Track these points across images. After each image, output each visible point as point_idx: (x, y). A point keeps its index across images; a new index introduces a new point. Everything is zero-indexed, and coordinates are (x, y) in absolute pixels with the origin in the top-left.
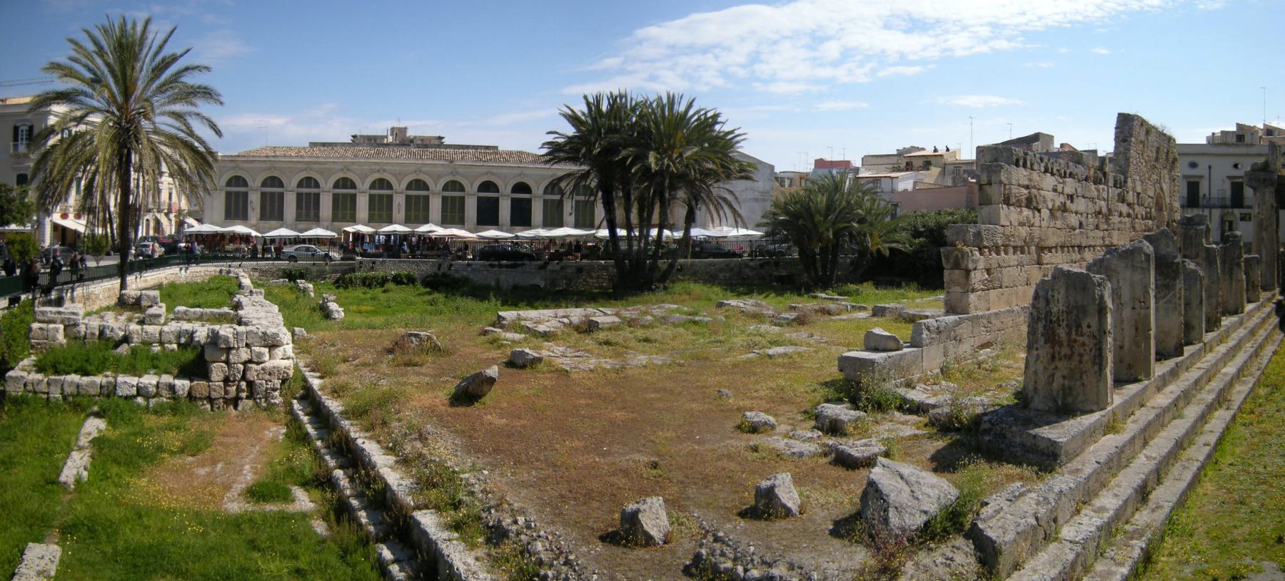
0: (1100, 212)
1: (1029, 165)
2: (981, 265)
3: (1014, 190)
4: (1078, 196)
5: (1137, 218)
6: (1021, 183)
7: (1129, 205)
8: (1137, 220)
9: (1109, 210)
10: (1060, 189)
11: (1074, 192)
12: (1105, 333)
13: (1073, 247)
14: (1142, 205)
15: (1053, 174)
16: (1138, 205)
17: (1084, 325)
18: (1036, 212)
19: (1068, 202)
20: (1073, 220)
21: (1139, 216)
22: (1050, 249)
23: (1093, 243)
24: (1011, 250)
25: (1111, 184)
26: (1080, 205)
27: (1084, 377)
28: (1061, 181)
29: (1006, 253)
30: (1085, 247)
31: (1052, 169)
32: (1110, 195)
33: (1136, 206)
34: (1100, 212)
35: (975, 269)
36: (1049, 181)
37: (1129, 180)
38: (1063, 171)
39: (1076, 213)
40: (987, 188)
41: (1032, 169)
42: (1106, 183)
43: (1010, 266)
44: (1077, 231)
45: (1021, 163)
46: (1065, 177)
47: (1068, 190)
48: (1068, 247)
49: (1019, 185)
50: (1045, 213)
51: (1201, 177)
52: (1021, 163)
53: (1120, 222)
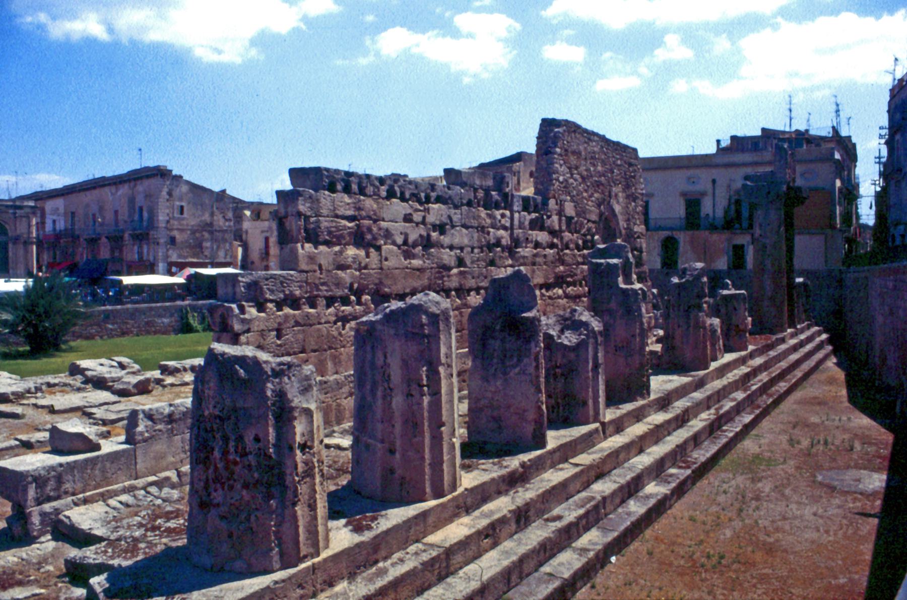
0: (498, 243)
3: (325, 223)
4: (453, 227)
5: (567, 248)
6: (339, 213)
7: (553, 233)
8: (567, 251)
10: (417, 217)
14: (577, 232)
15: (403, 199)
18: (372, 250)
19: (434, 235)
24: (322, 302)
26: (460, 236)
27: (253, 518)
28: (422, 208)
29: (313, 306)
30: (469, 291)
31: (402, 193)
32: (516, 222)
34: (498, 243)
35: (248, 331)
36: (398, 207)
37: (552, 202)
38: (423, 195)
39: (451, 248)
42: (509, 206)
43: (320, 323)
44: (455, 271)
49: (337, 216)
51: (703, 194)
52: (339, 187)
53: (535, 255)
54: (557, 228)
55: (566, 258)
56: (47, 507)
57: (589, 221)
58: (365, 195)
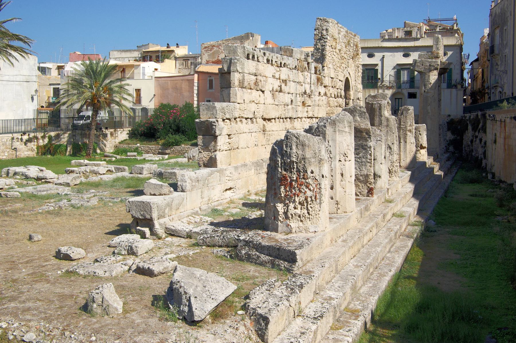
0: (305, 93)
1: (256, 59)
2: (225, 132)
9: (312, 91)
11: (287, 77)
12: (323, 177)
13: (286, 118)
15: (272, 65)
16: (332, 87)
17: (309, 172)
19: (283, 85)
20: (286, 98)
21: (333, 96)
22: (269, 120)
23: (300, 116)
25: (313, 71)
26: (292, 87)
30: (295, 118)
31: (272, 61)
32: (312, 80)
33: (331, 88)
34: (305, 93)
40: (226, 75)
41: (258, 61)
43: (244, 133)
44: (290, 107)
45: (251, 57)
46: (281, 66)
47: (283, 77)
48: (283, 118)
50: (268, 94)
51: (377, 65)
52: (251, 57)
54: (328, 85)
55: (331, 103)
56: (162, 221)
57: (340, 80)
58: (259, 62)
